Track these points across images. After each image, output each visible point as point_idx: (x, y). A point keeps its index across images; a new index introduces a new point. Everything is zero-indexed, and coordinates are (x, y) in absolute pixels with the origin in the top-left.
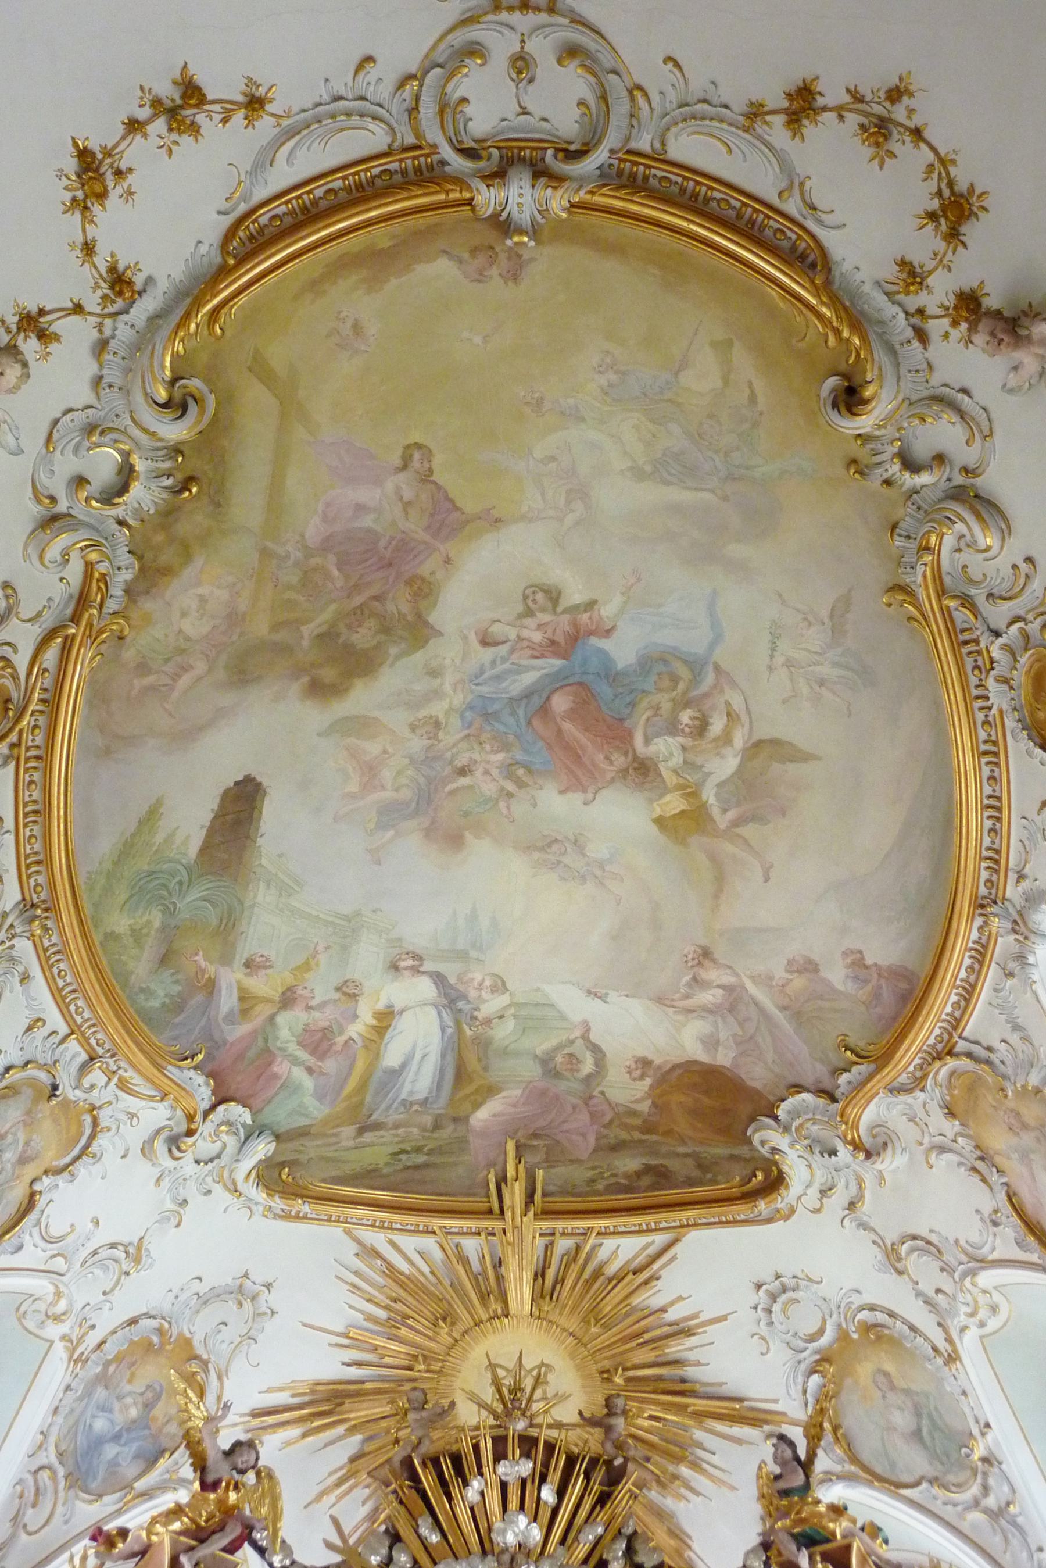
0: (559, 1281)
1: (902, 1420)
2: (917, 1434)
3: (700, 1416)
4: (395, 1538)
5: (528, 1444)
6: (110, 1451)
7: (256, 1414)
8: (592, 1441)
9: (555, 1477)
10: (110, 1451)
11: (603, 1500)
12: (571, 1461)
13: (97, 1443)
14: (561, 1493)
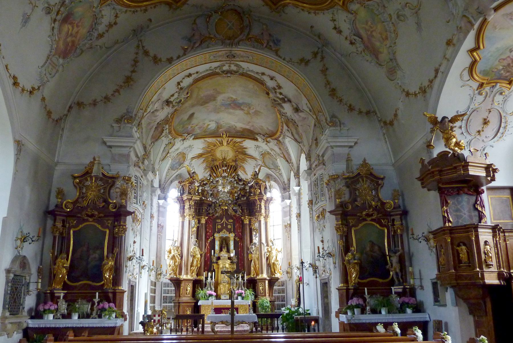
0: (230, 142)
1: (271, 162)
2: (273, 164)
3: (247, 157)
4: (211, 176)
5: (226, 166)
6: (175, 165)
7: (192, 158)
8: (234, 164)
9: (229, 168)
10: (175, 165)
11: (235, 171)
12: (231, 166)
13: (174, 165)
14: (230, 170)
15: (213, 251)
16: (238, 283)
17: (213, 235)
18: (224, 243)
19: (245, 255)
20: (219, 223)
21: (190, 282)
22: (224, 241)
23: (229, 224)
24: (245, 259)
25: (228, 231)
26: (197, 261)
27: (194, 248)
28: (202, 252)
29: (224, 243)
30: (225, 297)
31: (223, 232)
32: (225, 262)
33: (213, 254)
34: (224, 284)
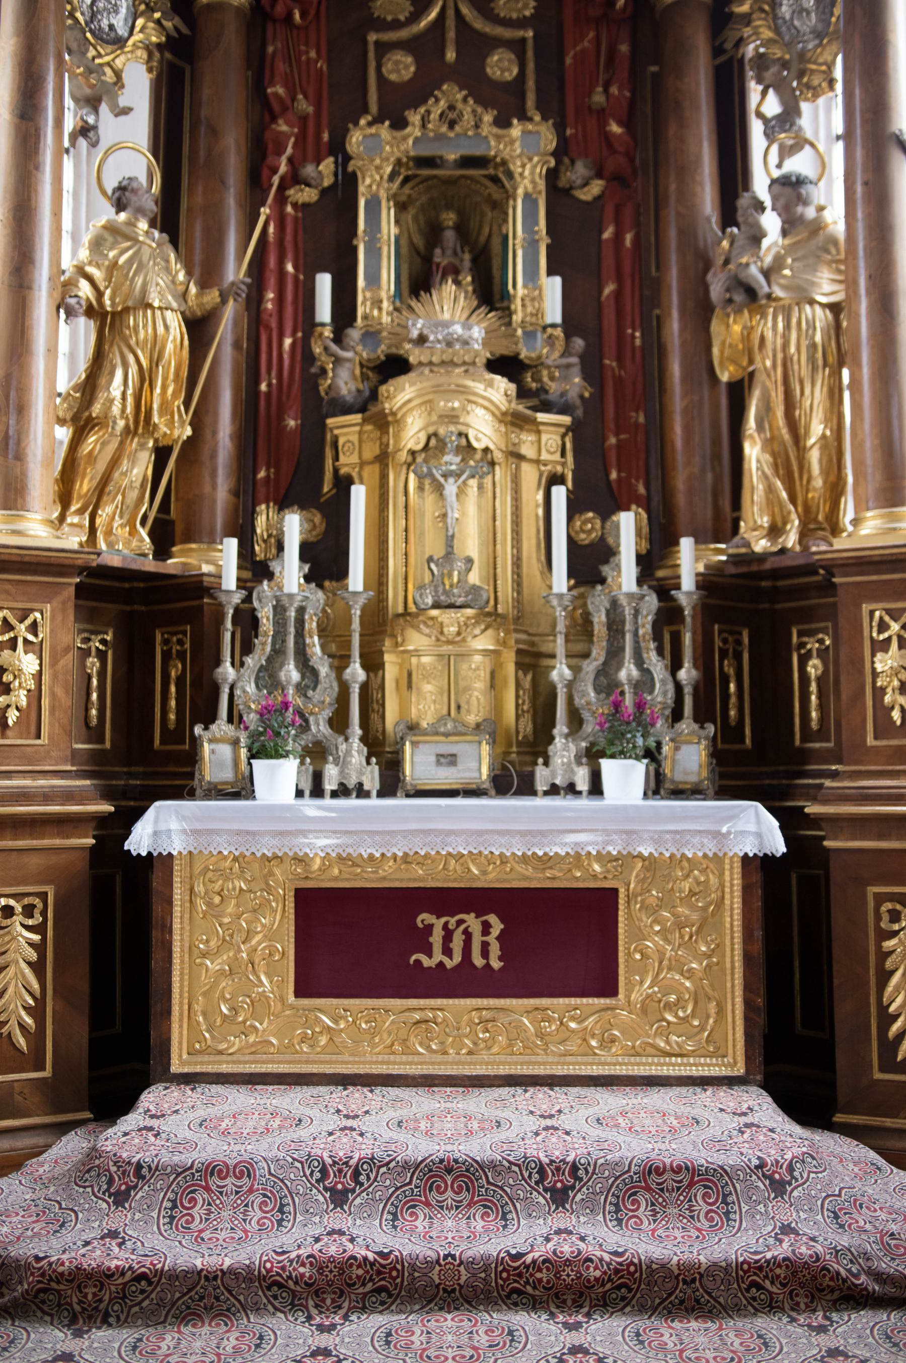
15: (324, 283)
16: (600, 619)
17: (338, 149)
18: (450, 236)
19: (674, 325)
20: (396, 25)
21: (49, 593)
22: (449, 218)
23: (496, 43)
24: (675, 369)
25: (484, 102)
26: (146, 378)
27: (111, 228)
28: (212, 297)
29: (450, 236)
30: (451, 760)
31: (437, 109)
32: (462, 391)
33: (324, 311)
34: (450, 620)
